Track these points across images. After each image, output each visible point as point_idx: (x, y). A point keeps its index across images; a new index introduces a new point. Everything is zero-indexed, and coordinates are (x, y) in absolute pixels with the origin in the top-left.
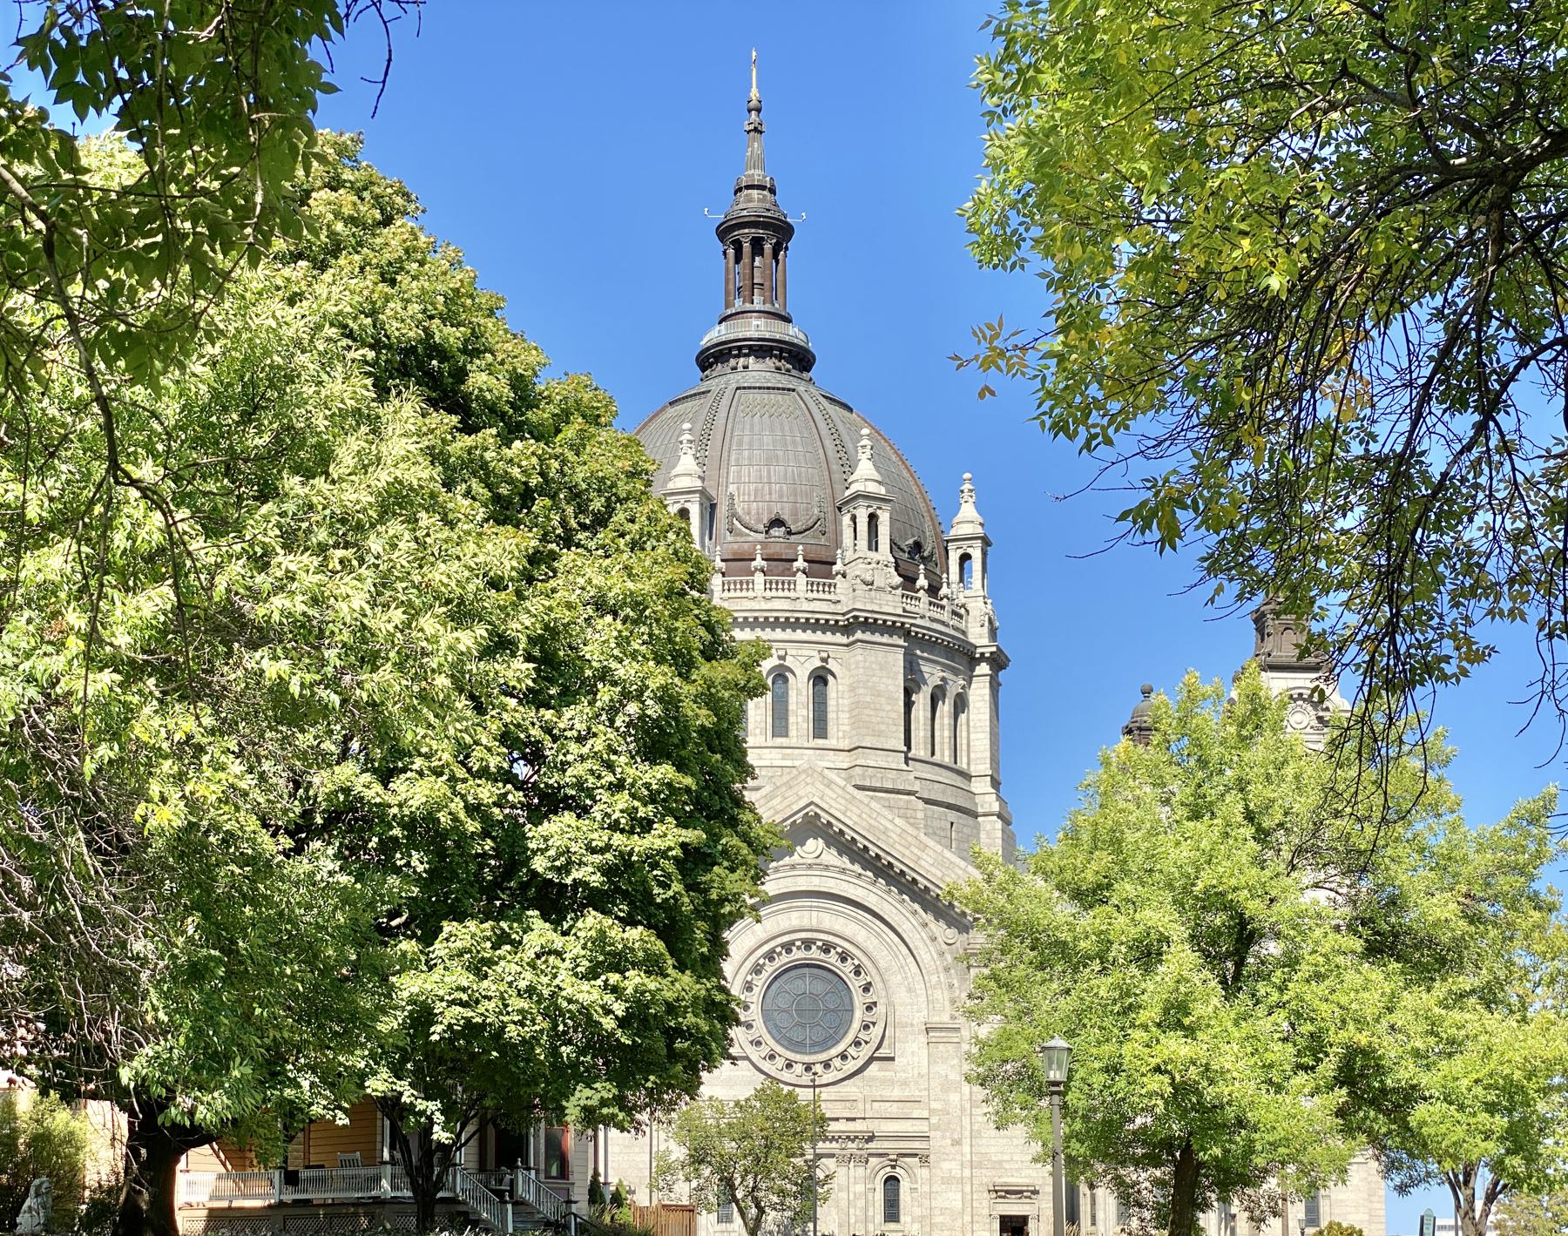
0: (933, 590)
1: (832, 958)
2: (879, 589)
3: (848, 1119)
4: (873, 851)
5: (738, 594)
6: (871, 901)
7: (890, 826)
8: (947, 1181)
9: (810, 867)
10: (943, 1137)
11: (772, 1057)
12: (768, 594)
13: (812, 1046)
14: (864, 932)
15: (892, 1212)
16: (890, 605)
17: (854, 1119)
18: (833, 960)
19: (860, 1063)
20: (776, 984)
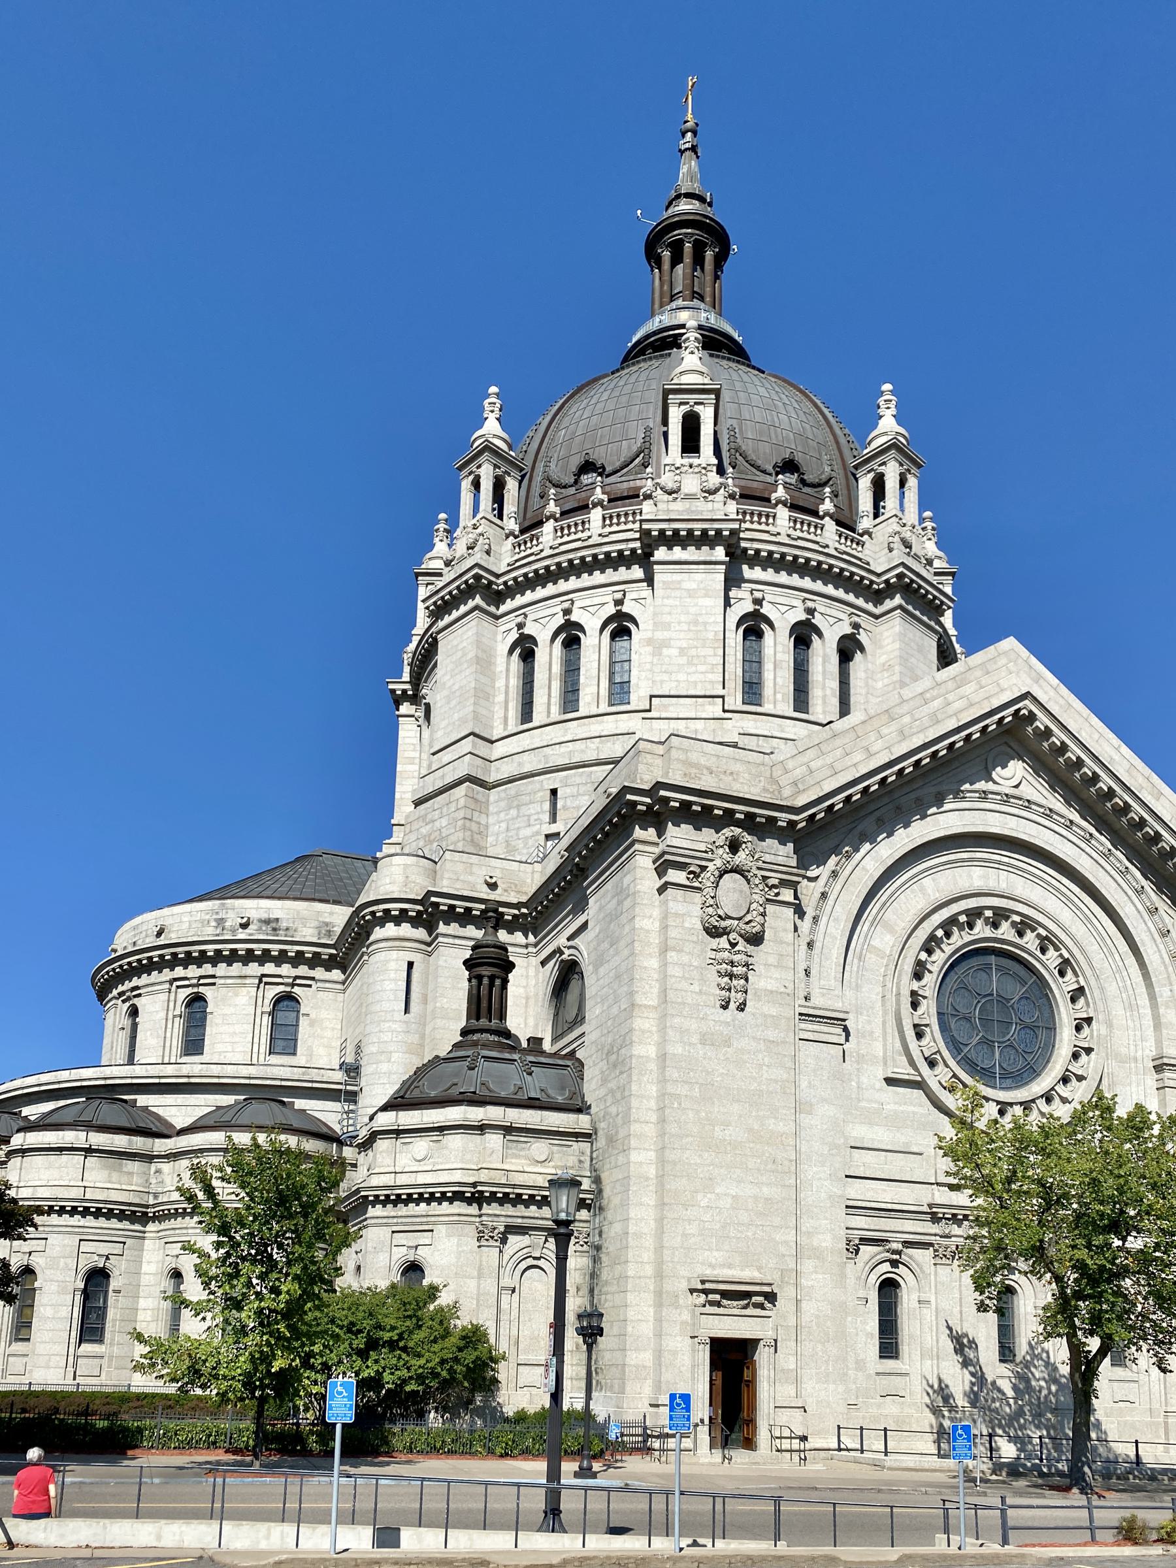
9: (1007, 799)
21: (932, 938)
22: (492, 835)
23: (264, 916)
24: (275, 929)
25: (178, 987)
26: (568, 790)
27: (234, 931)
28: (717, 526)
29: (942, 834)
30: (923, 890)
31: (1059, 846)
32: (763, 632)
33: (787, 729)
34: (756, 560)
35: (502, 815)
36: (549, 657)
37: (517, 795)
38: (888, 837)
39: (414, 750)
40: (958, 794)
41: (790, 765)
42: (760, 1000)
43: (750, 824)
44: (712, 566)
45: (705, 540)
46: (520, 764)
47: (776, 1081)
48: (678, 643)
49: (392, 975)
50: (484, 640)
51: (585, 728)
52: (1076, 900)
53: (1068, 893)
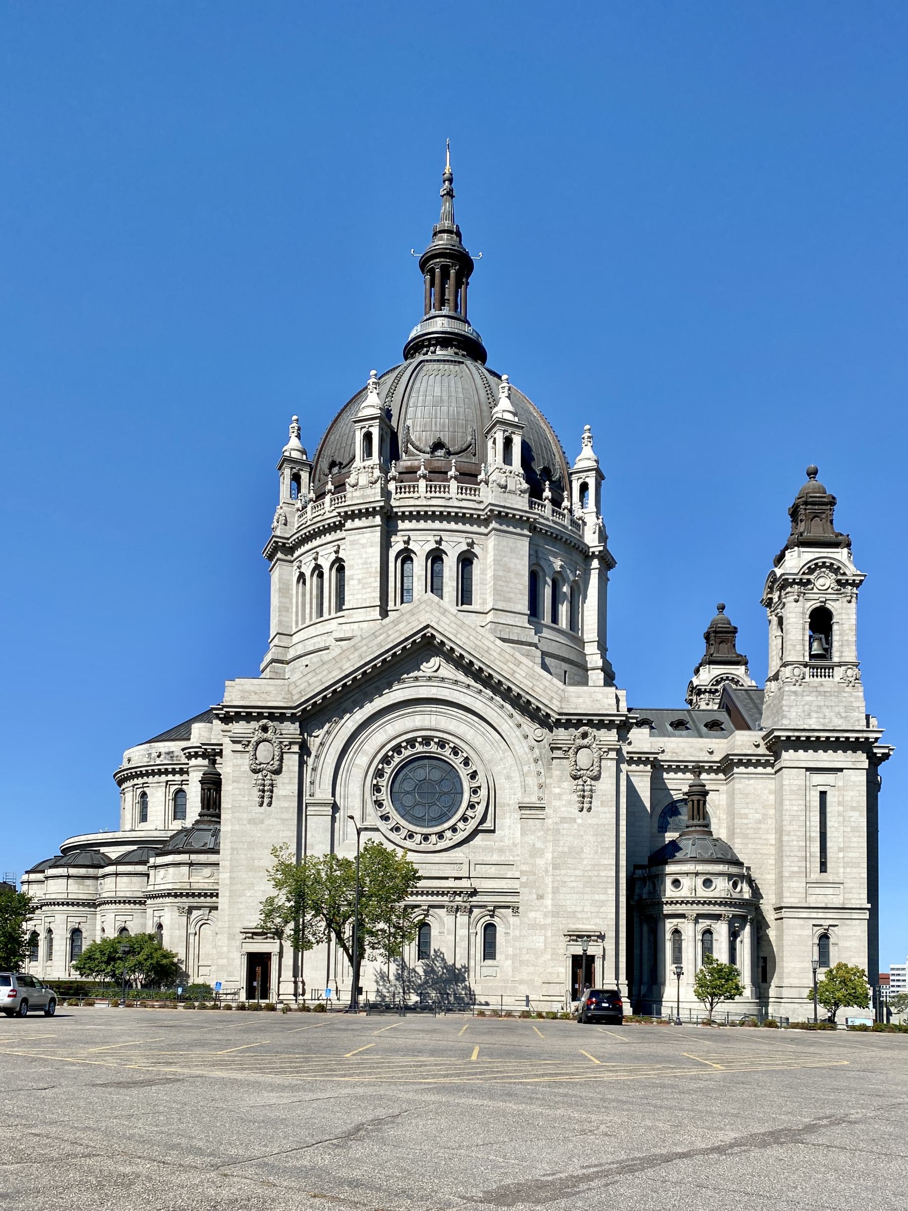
0: (556, 502)
1: (447, 752)
2: (510, 492)
3: (456, 878)
4: (477, 665)
5: (407, 495)
6: (477, 706)
7: (492, 647)
8: (533, 926)
9: (430, 678)
10: (530, 893)
11: (397, 829)
12: (429, 495)
13: (430, 821)
14: (472, 732)
15: (489, 951)
16: (520, 503)
17: (460, 878)
18: (447, 754)
19: (466, 834)
20: (403, 772)
21: (386, 756)
28: (373, 505)
29: (391, 703)
30: (386, 731)
31: (463, 699)
34: (404, 517)
36: (312, 583)
38: (360, 709)
40: (400, 681)
41: (298, 683)
42: (279, 800)
43: (271, 717)
45: (368, 514)
47: (286, 837)
50: (283, 577)
52: (477, 725)
53: (472, 722)
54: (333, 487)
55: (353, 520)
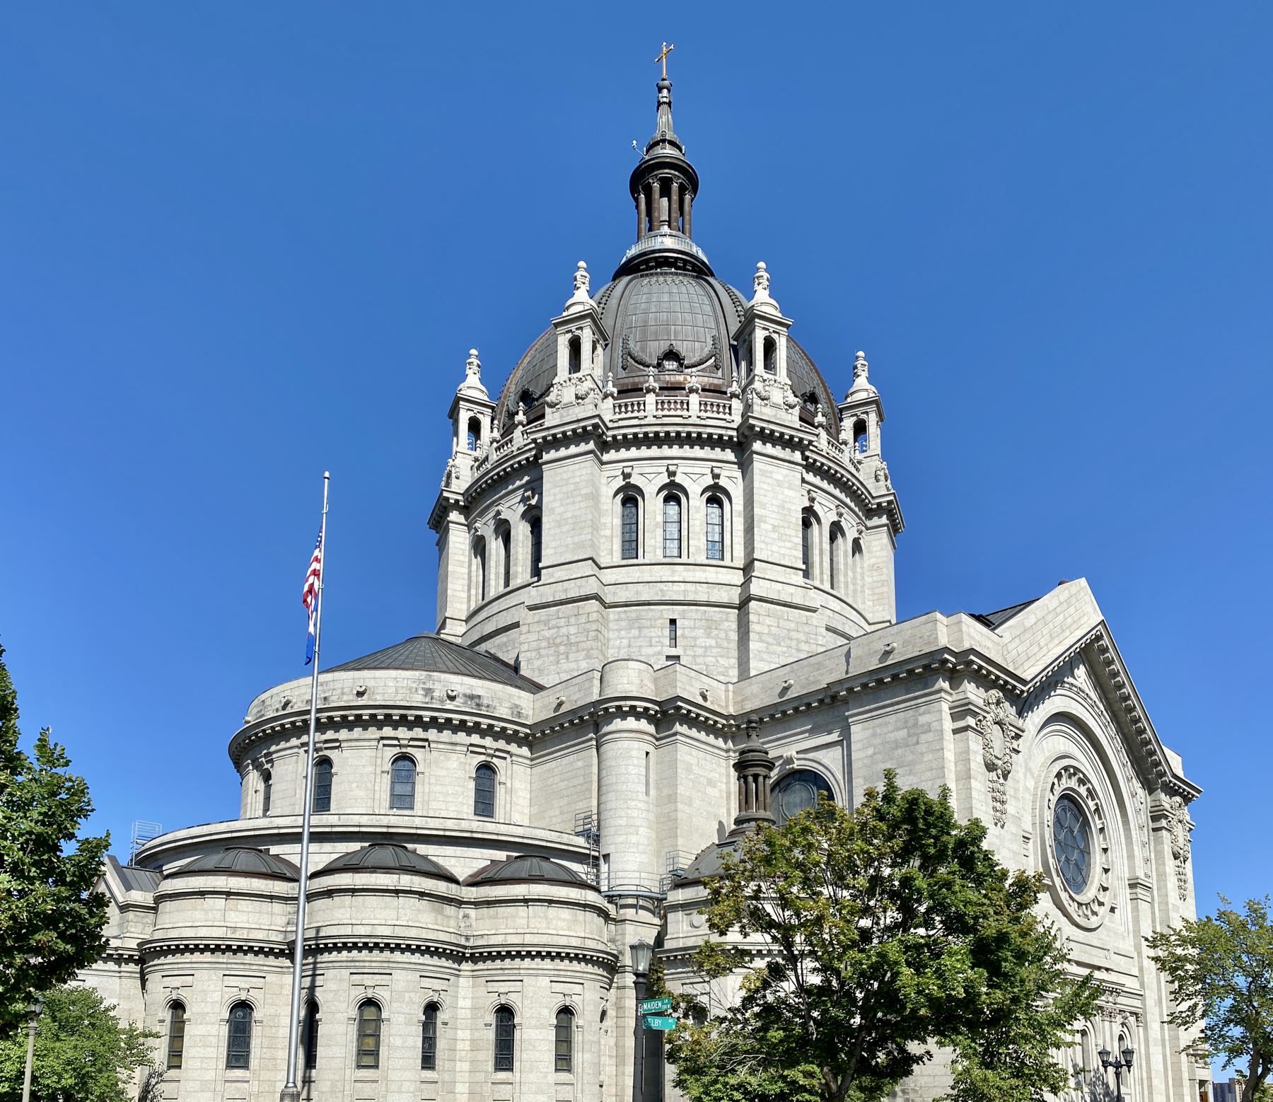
22: (613, 648)
23: (468, 692)
24: (478, 705)
25: (384, 745)
26: (686, 623)
27: (442, 702)
32: (811, 524)
33: (830, 603)
35: (623, 633)
37: (638, 619)
39: (463, 555)
44: (793, 466)
46: (637, 592)
48: (772, 521)
49: (636, 762)
51: (690, 574)
54: (615, 390)
55: (764, 444)
